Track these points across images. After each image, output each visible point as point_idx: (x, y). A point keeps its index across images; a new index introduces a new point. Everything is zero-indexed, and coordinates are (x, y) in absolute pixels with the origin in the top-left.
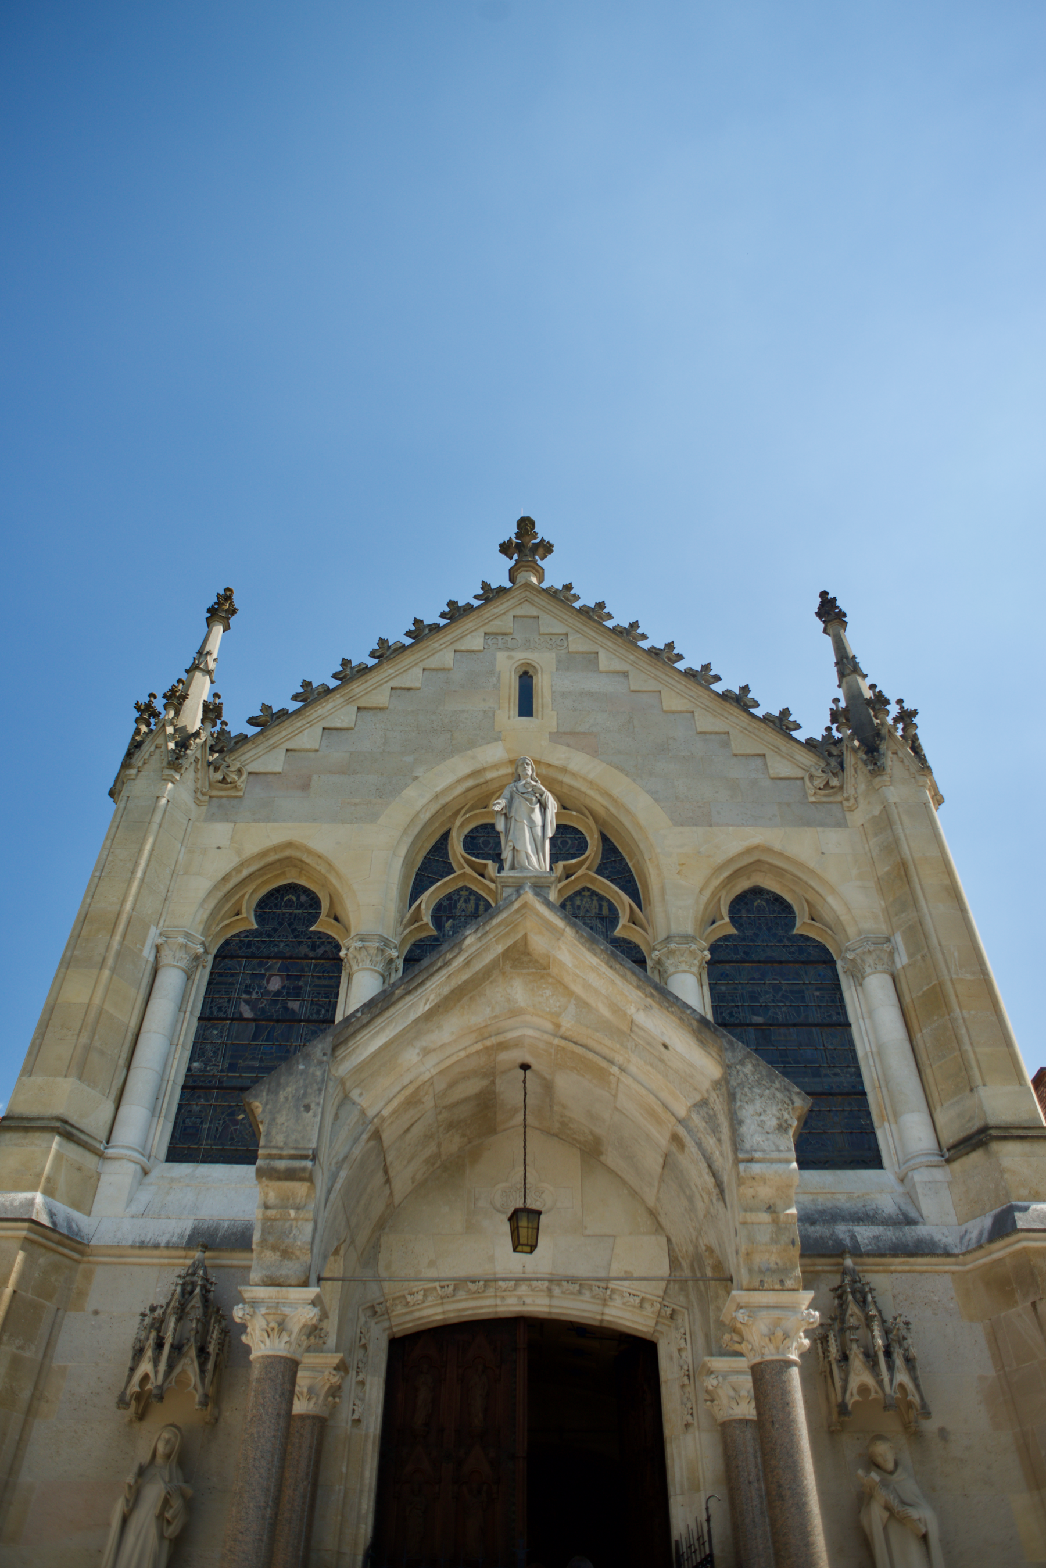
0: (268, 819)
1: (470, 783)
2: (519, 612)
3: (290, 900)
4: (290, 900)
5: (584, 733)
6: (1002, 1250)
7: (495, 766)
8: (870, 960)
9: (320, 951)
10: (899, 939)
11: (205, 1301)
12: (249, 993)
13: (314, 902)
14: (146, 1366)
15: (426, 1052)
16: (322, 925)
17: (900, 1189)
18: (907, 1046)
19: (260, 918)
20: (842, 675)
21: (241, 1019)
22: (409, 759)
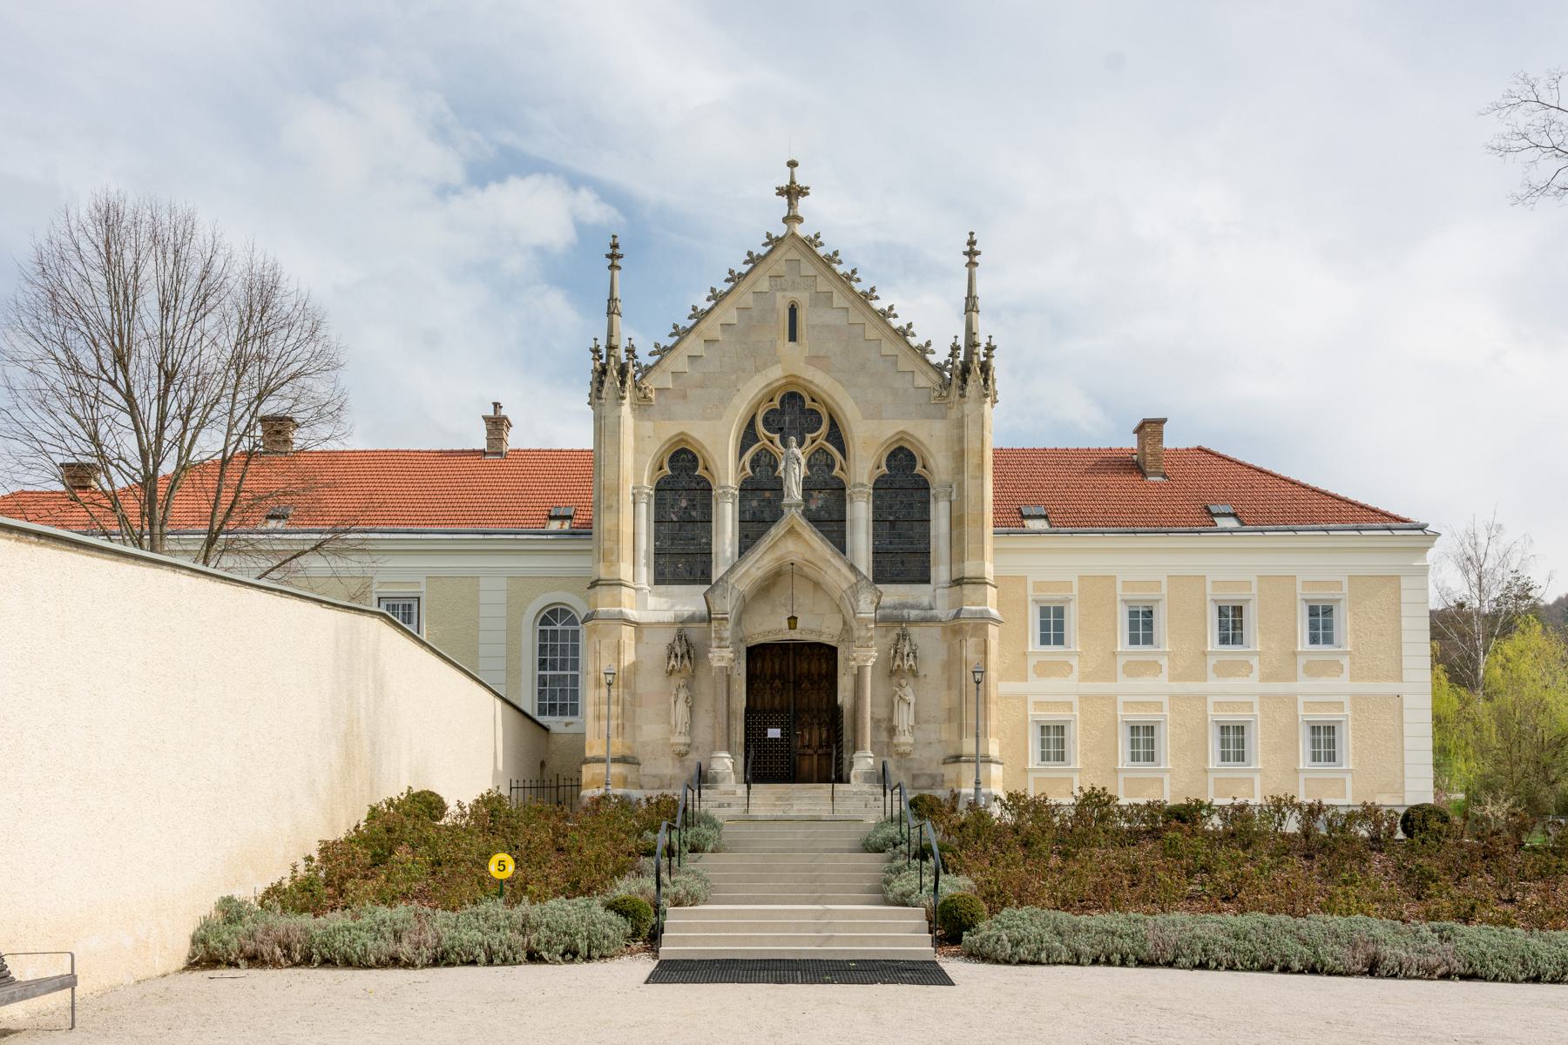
0: (669, 419)
1: (765, 391)
2: (789, 256)
3: (684, 458)
4: (684, 458)
5: (823, 357)
6: (956, 622)
7: (777, 380)
8: (942, 494)
9: (701, 485)
10: (954, 486)
11: (686, 640)
12: (673, 508)
13: (695, 459)
14: (673, 662)
15: (759, 568)
16: (700, 471)
17: (933, 594)
18: (948, 536)
19: (672, 468)
20: (966, 311)
21: (672, 521)
22: (734, 377)
